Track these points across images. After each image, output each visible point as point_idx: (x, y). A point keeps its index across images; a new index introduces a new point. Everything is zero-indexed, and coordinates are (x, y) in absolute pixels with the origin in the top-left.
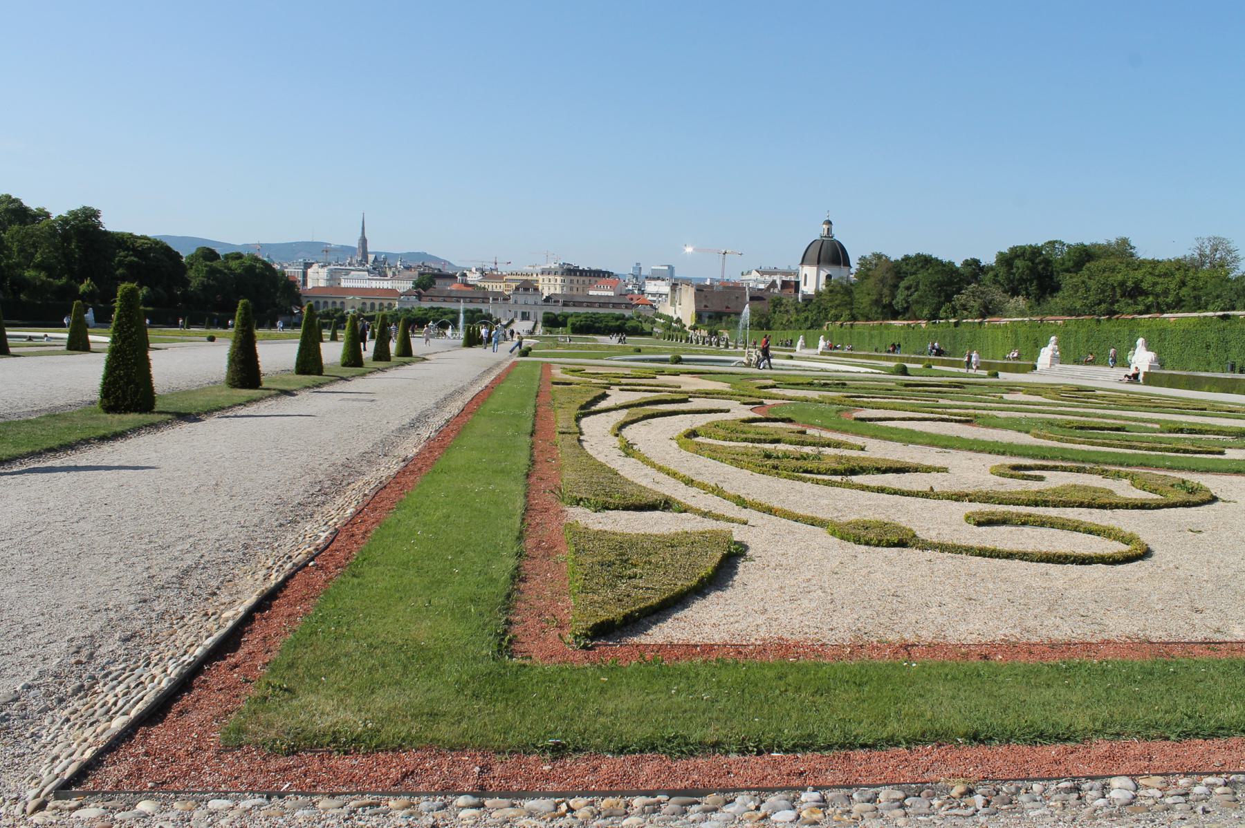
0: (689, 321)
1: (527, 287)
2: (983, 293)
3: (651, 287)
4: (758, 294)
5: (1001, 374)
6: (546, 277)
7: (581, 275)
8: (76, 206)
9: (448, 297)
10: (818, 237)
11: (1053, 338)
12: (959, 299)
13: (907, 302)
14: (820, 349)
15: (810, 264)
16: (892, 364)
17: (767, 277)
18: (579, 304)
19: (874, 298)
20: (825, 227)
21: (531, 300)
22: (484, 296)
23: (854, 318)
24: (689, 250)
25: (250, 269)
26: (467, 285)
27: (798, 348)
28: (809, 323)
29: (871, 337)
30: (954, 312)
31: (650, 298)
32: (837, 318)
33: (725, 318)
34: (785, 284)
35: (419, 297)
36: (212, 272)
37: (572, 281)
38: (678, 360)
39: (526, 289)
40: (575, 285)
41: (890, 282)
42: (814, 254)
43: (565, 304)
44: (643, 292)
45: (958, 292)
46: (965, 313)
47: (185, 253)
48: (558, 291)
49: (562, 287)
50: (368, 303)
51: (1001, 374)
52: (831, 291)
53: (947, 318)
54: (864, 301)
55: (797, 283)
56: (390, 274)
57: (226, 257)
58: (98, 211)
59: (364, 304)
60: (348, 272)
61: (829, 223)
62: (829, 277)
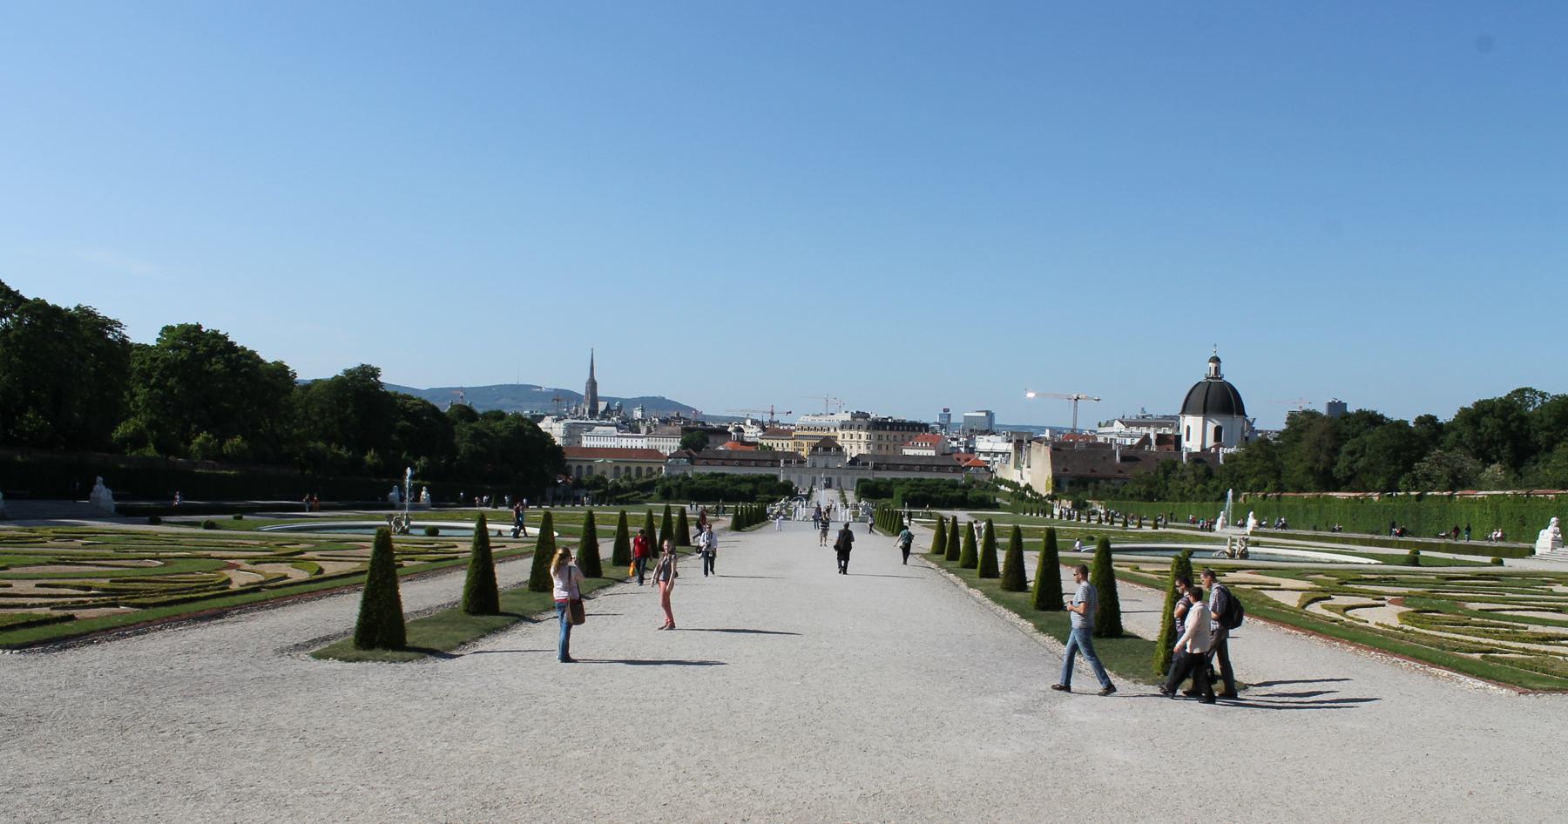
1: (827, 446)
2: (1449, 460)
3: (983, 444)
4: (1131, 453)
5: (1506, 561)
7: (891, 429)
8: (353, 364)
10: (1202, 379)
11: (1553, 519)
12: (1421, 467)
13: (1351, 470)
14: (1249, 529)
15: (1194, 413)
16: (1406, 552)
17: (1134, 429)
18: (895, 467)
19: (1308, 464)
22: (774, 458)
23: (1280, 488)
24: (1031, 395)
25: (520, 430)
26: (744, 443)
29: (1307, 512)
30: (1415, 484)
31: (982, 458)
32: (1260, 487)
33: (1091, 485)
34: (1161, 439)
35: (692, 460)
36: (477, 436)
37: (880, 437)
38: (1244, 555)
39: (827, 449)
40: (884, 443)
41: (1328, 445)
42: (1199, 400)
43: (877, 467)
44: (972, 451)
45: (1420, 459)
46: (1429, 484)
47: (445, 408)
48: (863, 451)
50: (623, 467)
51: (1506, 561)
52: (1248, 455)
53: (1408, 490)
54: (1295, 467)
55: (1179, 438)
56: (644, 431)
57: (485, 416)
58: (378, 370)
59: (617, 468)
60: (590, 427)
61: (1216, 360)
62: (1218, 430)
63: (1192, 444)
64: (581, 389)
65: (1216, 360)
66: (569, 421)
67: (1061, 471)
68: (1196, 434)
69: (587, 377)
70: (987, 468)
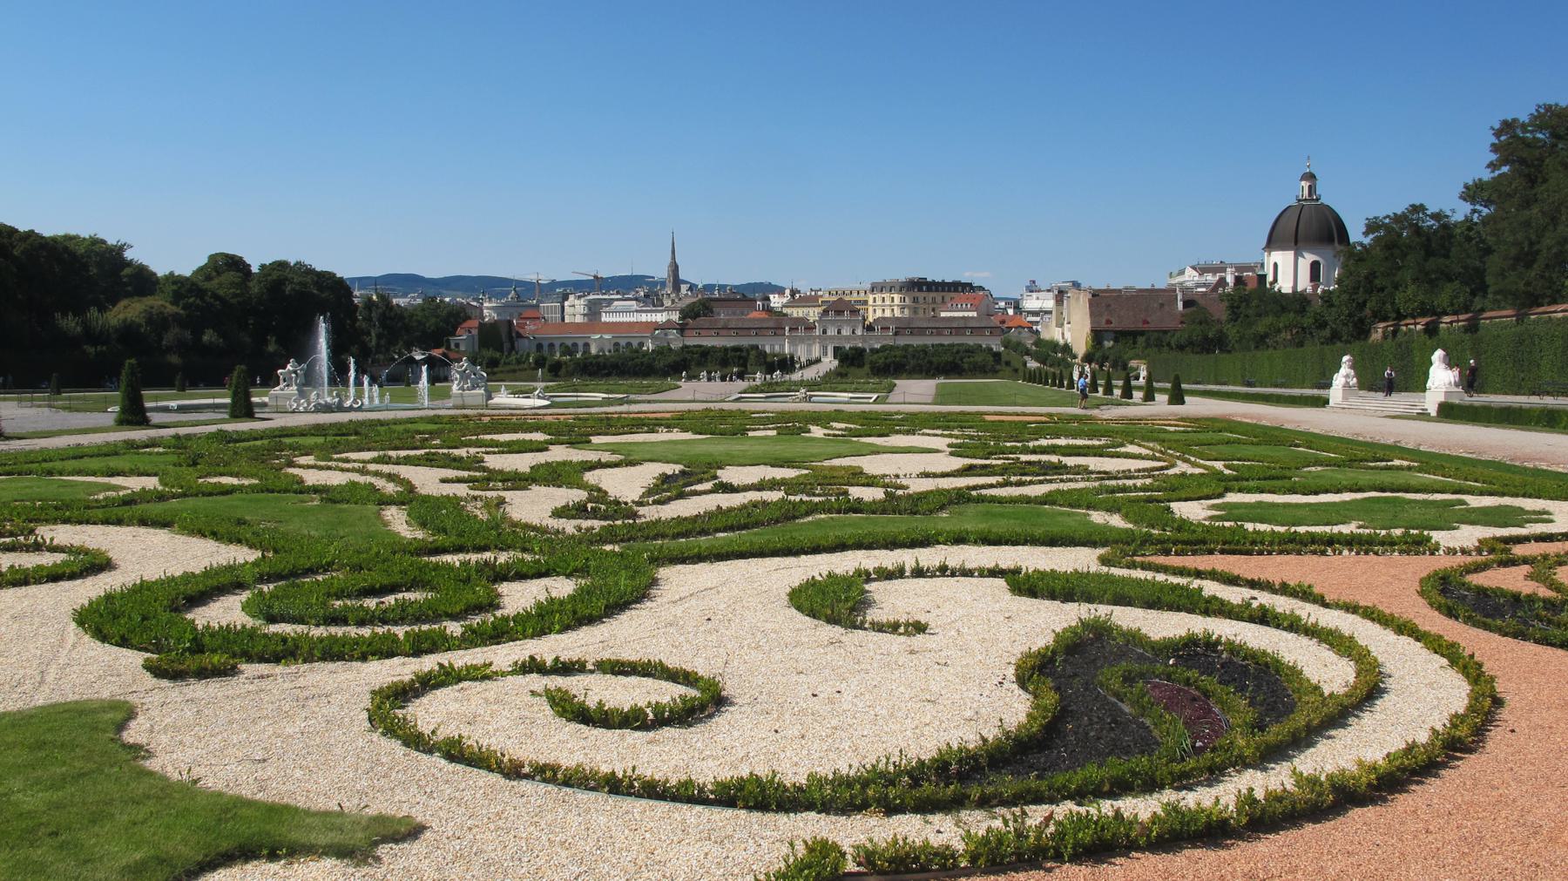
0: (1080, 347)
6: (878, 296)
7: (929, 290)
10: (1293, 202)
18: (921, 331)
20: (1305, 184)
27: (1336, 393)
28: (1327, 332)
31: (1031, 318)
35: (682, 329)
37: (915, 300)
39: (839, 312)
61: (1310, 177)
62: (1315, 267)
64: (661, 272)
65: (1310, 177)
67: (1103, 325)
69: (669, 260)
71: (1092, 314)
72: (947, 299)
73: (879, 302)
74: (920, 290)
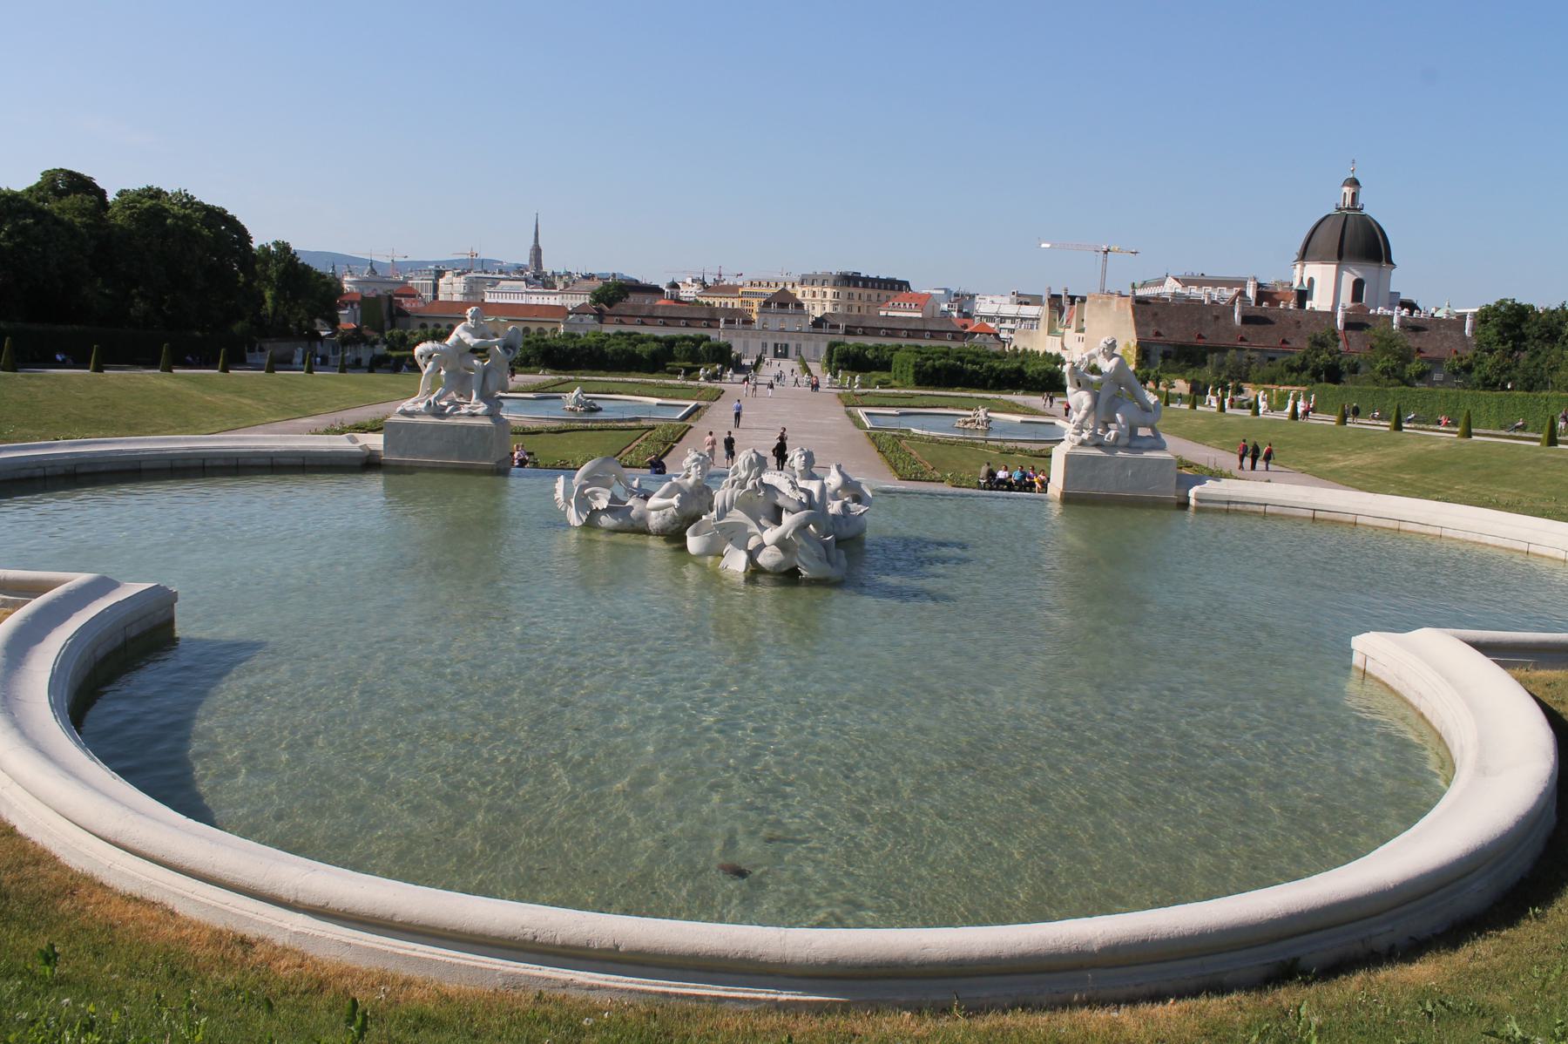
7: (865, 286)
9: (648, 318)
10: (1332, 211)
15: (1323, 259)
20: (1348, 190)
21: (790, 323)
26: (678, 301)
35: (601, 317)
37: (850, 296)
40: (856, 303)
42: (1329, 238)
44: (967, 316)
48: (829, 309)
49: (835, 305)
61: (1354, 183)
62: (1358, 285)
63: (1320, 301)
65: (1354, 183)
66: (473, 275)
68: (1327, 287)
69: (532, 243)
70: (997, 335)
71: (1137, 324)
72: (883, 298)
73: (819, 297)
74: (856, 285)
